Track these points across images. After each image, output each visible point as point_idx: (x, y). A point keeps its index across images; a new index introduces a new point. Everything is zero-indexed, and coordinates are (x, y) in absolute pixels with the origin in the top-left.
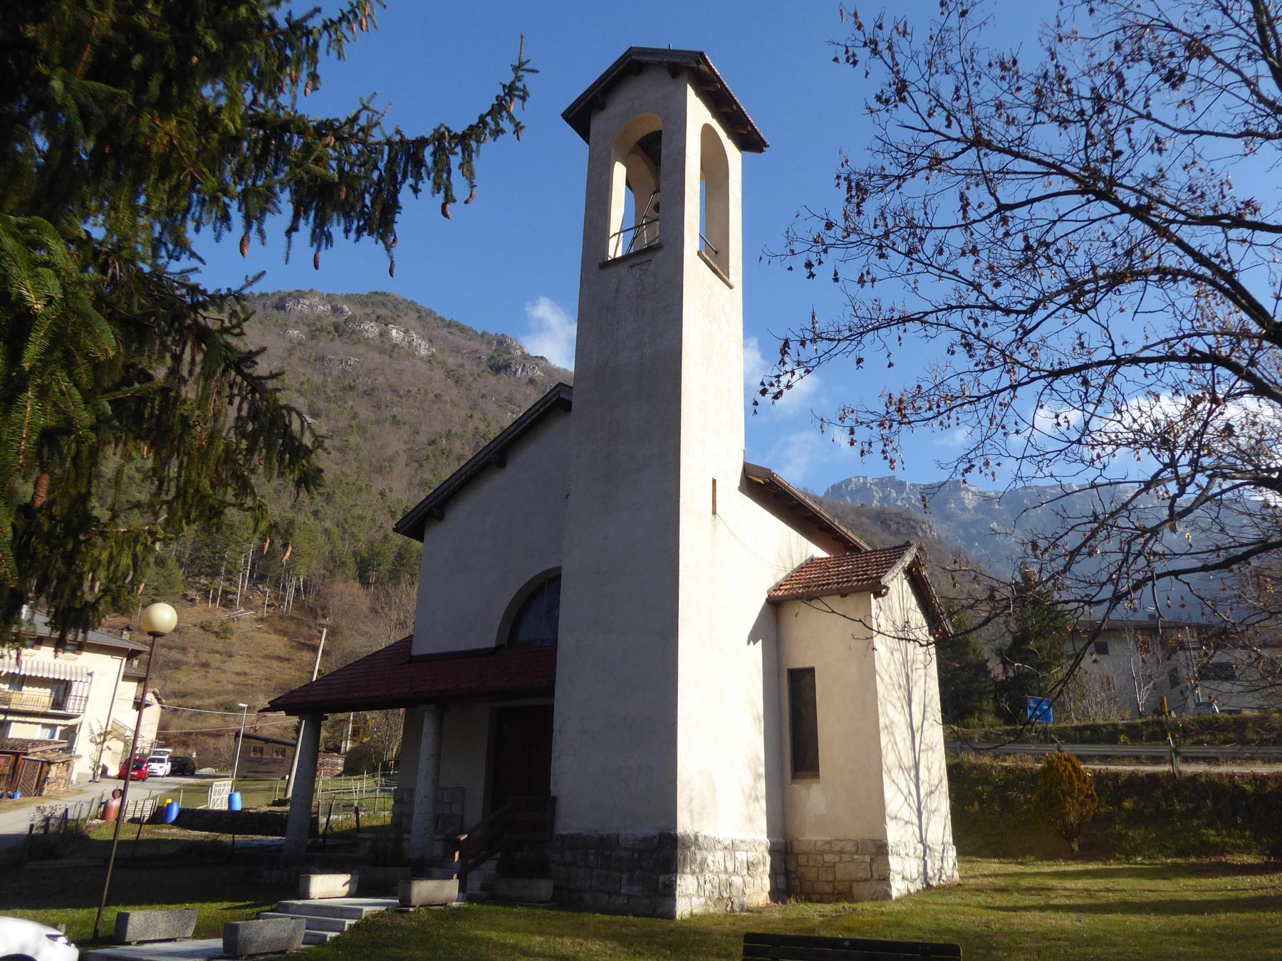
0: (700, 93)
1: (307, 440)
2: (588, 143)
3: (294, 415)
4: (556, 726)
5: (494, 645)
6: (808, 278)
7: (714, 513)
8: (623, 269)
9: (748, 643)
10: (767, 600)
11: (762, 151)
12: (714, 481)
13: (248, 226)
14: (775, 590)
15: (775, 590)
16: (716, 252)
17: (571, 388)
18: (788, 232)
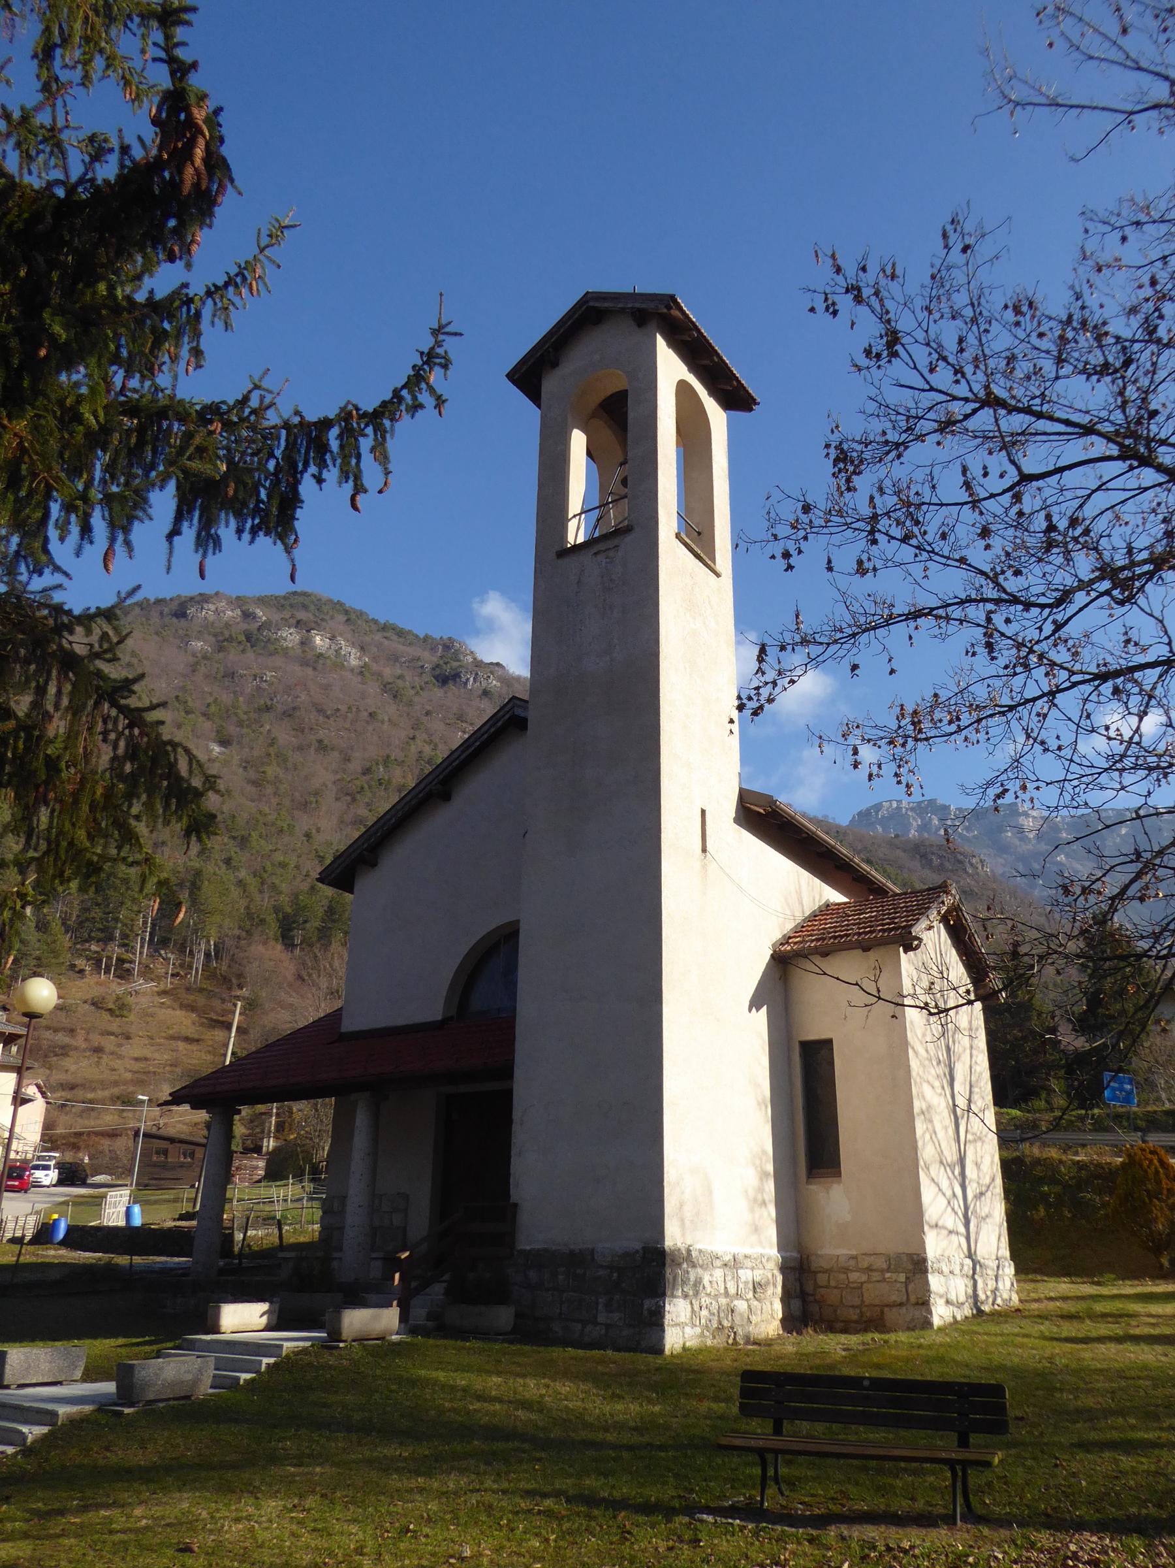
0: (673, 343)
1: (197, 782)
2: (539, 407)
3: (180, 750)
4: (516, 1115)
5: (439, 1018)
6: (786, 570)
7: (704, 850)
8: (586, 558)
9: (750, 1011)
10: (772, 956)
11: (751, 410)
12: (703, 812)
13: (112, 540)
14: (782, 944)
15: (782, 944)
16: (699, 534)
17: (526, 702)
18: (769, 513)
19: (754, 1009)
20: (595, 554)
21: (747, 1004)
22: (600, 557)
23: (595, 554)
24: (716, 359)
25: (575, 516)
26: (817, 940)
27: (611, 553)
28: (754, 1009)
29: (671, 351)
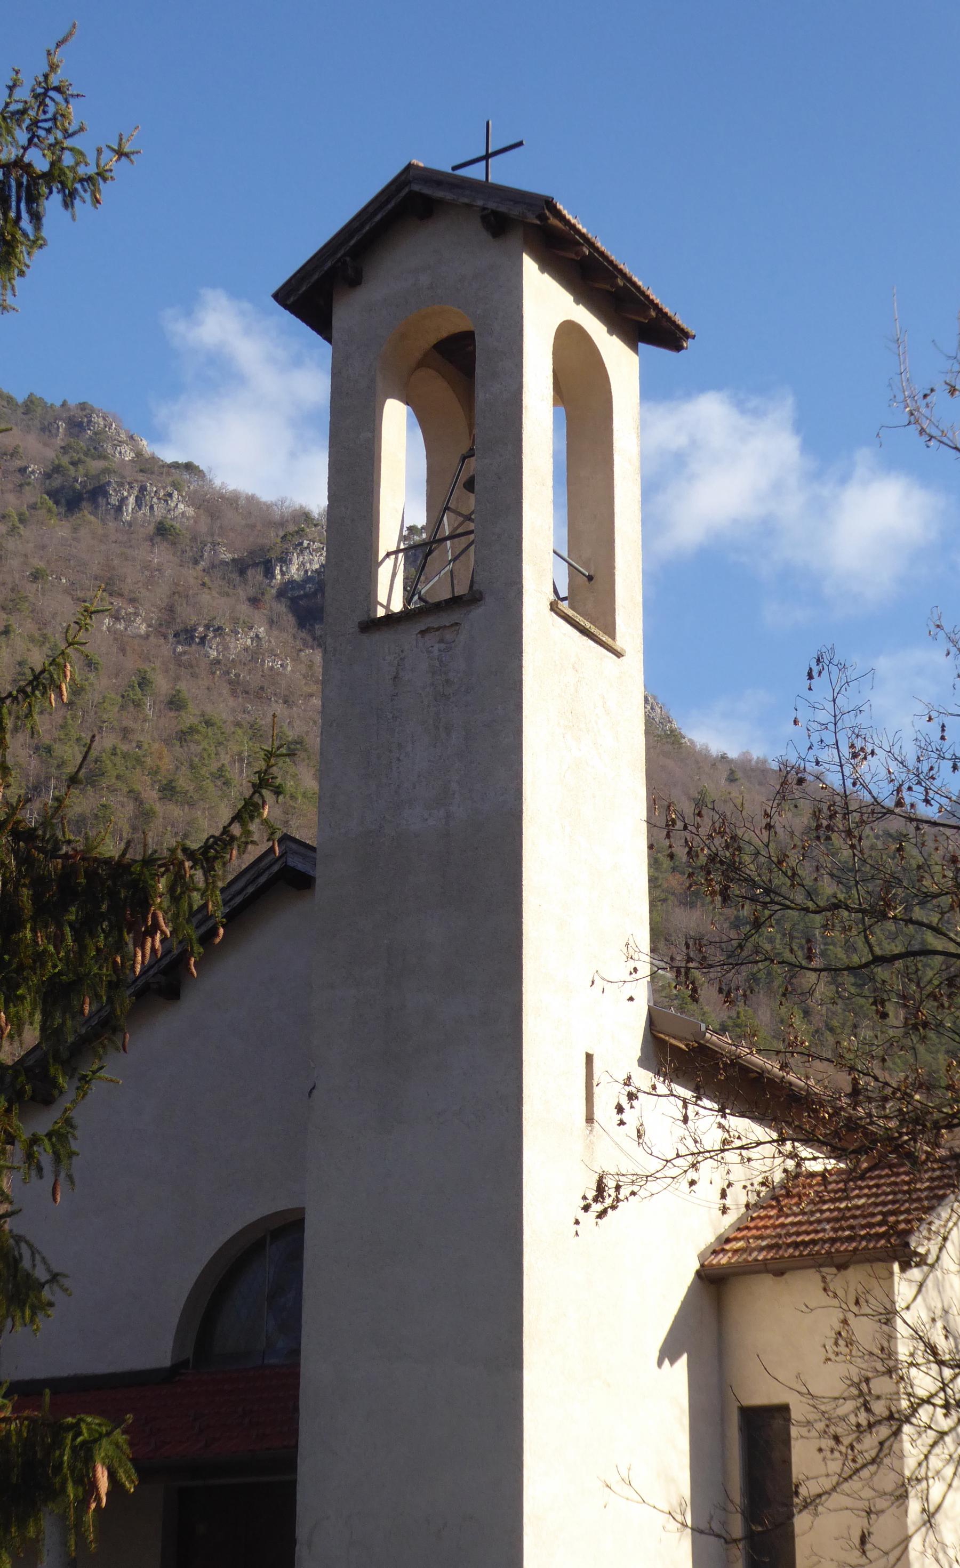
0: (548, 264)
1: (41, 1274)
2: (329, 339)
3: (23, 1246)
4: (302, 1532)
5: (167, 1363)
6: (619, 1125)
7: (590, 1119)
8: (408, 637)
9: (660, 1364)
10: (698, 1273)
11: (678, 348)
12: (589, 1058)
13: (57, 1175)
14: (715, 1252)
15: (715, 1252)
16: (590, 578)
17: (313, 849)
18: (627, 945)
19: (667, 1362)
20: (423, 633)
21: (656, 1354)
22: (431, 639)
23: (423, 633)
24: (620, 282)
25: (388, 555)
26: (769, 1247)
27: (448, 636)
28: (667, 1362)
29: (546, 277)
